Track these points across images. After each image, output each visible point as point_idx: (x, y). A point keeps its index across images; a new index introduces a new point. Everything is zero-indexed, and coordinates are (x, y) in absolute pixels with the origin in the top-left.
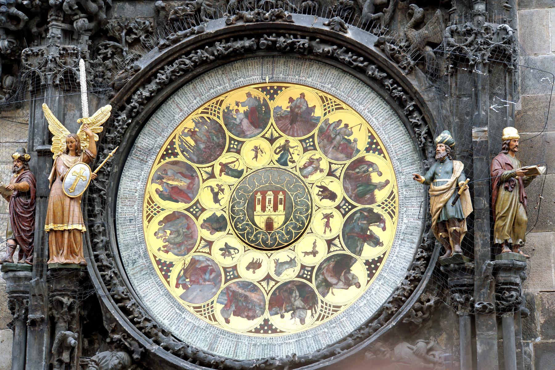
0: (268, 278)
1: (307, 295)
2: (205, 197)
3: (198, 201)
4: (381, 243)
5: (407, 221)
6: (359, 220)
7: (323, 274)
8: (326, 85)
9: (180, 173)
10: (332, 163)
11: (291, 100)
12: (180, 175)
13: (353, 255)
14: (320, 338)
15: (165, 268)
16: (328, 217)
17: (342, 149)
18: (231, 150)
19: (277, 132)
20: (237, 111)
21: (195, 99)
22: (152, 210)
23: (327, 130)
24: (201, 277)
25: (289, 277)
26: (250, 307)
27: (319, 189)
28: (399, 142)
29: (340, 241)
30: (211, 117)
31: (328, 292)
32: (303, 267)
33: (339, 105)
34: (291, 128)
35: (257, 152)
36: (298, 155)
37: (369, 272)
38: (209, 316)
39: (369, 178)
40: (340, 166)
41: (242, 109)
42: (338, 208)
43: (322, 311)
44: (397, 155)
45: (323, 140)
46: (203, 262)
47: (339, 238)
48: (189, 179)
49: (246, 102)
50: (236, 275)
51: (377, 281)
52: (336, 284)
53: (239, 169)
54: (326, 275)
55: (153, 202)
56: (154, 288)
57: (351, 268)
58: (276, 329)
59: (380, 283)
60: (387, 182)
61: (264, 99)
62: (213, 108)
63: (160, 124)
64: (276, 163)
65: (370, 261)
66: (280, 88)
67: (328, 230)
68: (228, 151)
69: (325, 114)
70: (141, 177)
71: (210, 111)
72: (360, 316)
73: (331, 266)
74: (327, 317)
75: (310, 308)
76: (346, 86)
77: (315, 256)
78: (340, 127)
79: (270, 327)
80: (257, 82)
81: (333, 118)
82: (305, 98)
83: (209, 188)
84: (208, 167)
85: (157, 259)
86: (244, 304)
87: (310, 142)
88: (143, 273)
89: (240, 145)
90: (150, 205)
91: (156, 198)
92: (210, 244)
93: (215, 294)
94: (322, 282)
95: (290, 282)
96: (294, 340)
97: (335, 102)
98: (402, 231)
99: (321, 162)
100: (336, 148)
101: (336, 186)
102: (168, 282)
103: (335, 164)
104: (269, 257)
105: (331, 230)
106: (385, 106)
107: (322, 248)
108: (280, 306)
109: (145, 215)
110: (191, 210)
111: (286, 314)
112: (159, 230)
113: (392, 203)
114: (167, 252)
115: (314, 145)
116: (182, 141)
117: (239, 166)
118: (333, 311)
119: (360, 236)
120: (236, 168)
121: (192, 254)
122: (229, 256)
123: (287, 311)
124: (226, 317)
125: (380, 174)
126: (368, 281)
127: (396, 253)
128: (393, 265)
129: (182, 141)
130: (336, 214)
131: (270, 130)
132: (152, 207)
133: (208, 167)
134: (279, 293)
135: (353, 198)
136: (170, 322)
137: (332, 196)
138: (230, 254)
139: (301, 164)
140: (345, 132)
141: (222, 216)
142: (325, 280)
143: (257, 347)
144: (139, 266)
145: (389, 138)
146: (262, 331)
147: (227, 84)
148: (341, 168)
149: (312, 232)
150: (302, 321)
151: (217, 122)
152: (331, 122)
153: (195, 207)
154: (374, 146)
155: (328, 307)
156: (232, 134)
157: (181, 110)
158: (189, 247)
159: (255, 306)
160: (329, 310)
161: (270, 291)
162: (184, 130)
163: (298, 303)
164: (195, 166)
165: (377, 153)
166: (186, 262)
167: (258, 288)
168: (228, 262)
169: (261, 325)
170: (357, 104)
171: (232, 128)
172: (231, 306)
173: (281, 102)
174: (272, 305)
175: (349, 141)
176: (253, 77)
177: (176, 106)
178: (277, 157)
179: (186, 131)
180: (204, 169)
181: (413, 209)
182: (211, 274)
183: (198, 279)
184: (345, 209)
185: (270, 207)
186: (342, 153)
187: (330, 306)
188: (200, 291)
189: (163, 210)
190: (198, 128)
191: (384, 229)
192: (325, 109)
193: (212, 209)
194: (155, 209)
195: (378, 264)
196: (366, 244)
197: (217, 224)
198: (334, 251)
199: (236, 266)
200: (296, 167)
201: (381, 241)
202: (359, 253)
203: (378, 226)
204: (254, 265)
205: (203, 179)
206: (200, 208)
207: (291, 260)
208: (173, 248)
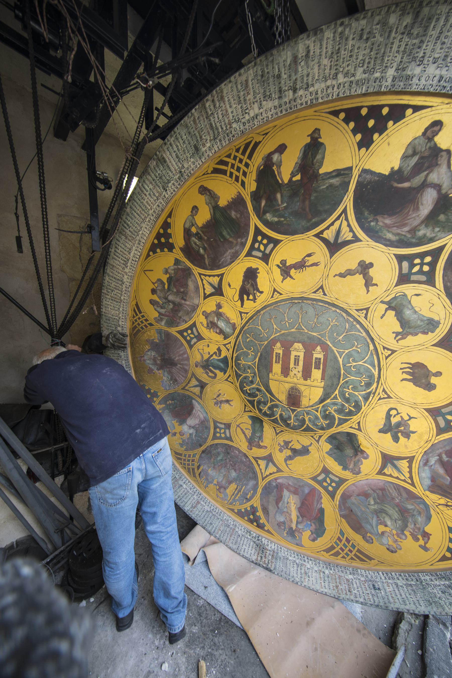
2: (304, 469)
3: (314, 479)
5: (256, 106)
6: (278, 210)
7: (414, 230)
9: (277, 502)
13: (352, 186)
21: (181, 486)
23: (167, 316)
25: (435, 300)
28: (145, 202)
29: (328, 228)
30: (196, 464)
32: (403, 279)
34: (180, 364)
35: (221, 402)
36: (208, 346)
40: (205, 282)
42: (266, 258)
44: (160, 195)
45: (180, 317)
47: (322, 232)
51: (415, 80)
53: (250, 422)
60: (203, 190)
64: (227, 374)
67: (311, 260)
70: (297, 561)
73: (388, 221)
76: (112, 308)
77: (371, 265)
83: (288, 462)
89: (218, 424)
92: (388, 459)
94: (437, 223)
100: (184, 295)
101: (234, 275)
103: (204, 289)
104: (393, 352)
105: (309, 255)
107: (348, 258)
113: (231, 161)
114: (426, 536)
115: (191, 328)
120: (250, 427)
125: (195, 209)
127: (329, 83)
133: (259, 465)
137: (251, 275)
139: (220, 338)
148: (207, 278)
149: (322, 287)
151: (200, 457)
154: (163, 240)
156: (208, 436)
158: (405, 495)
164: (262, 484)
170: (124, 286)
175: (170, 280)
180: (263, 471)
181: (230, 110)
184: (266, 246)
185: (297, 371)
186: (186, 285)
190: (213, 480)
196: (321, 171)
198: (351, 230)
199: (429, 411)
200: (225, 345)
201: (308, 140)
203: (279, 165)
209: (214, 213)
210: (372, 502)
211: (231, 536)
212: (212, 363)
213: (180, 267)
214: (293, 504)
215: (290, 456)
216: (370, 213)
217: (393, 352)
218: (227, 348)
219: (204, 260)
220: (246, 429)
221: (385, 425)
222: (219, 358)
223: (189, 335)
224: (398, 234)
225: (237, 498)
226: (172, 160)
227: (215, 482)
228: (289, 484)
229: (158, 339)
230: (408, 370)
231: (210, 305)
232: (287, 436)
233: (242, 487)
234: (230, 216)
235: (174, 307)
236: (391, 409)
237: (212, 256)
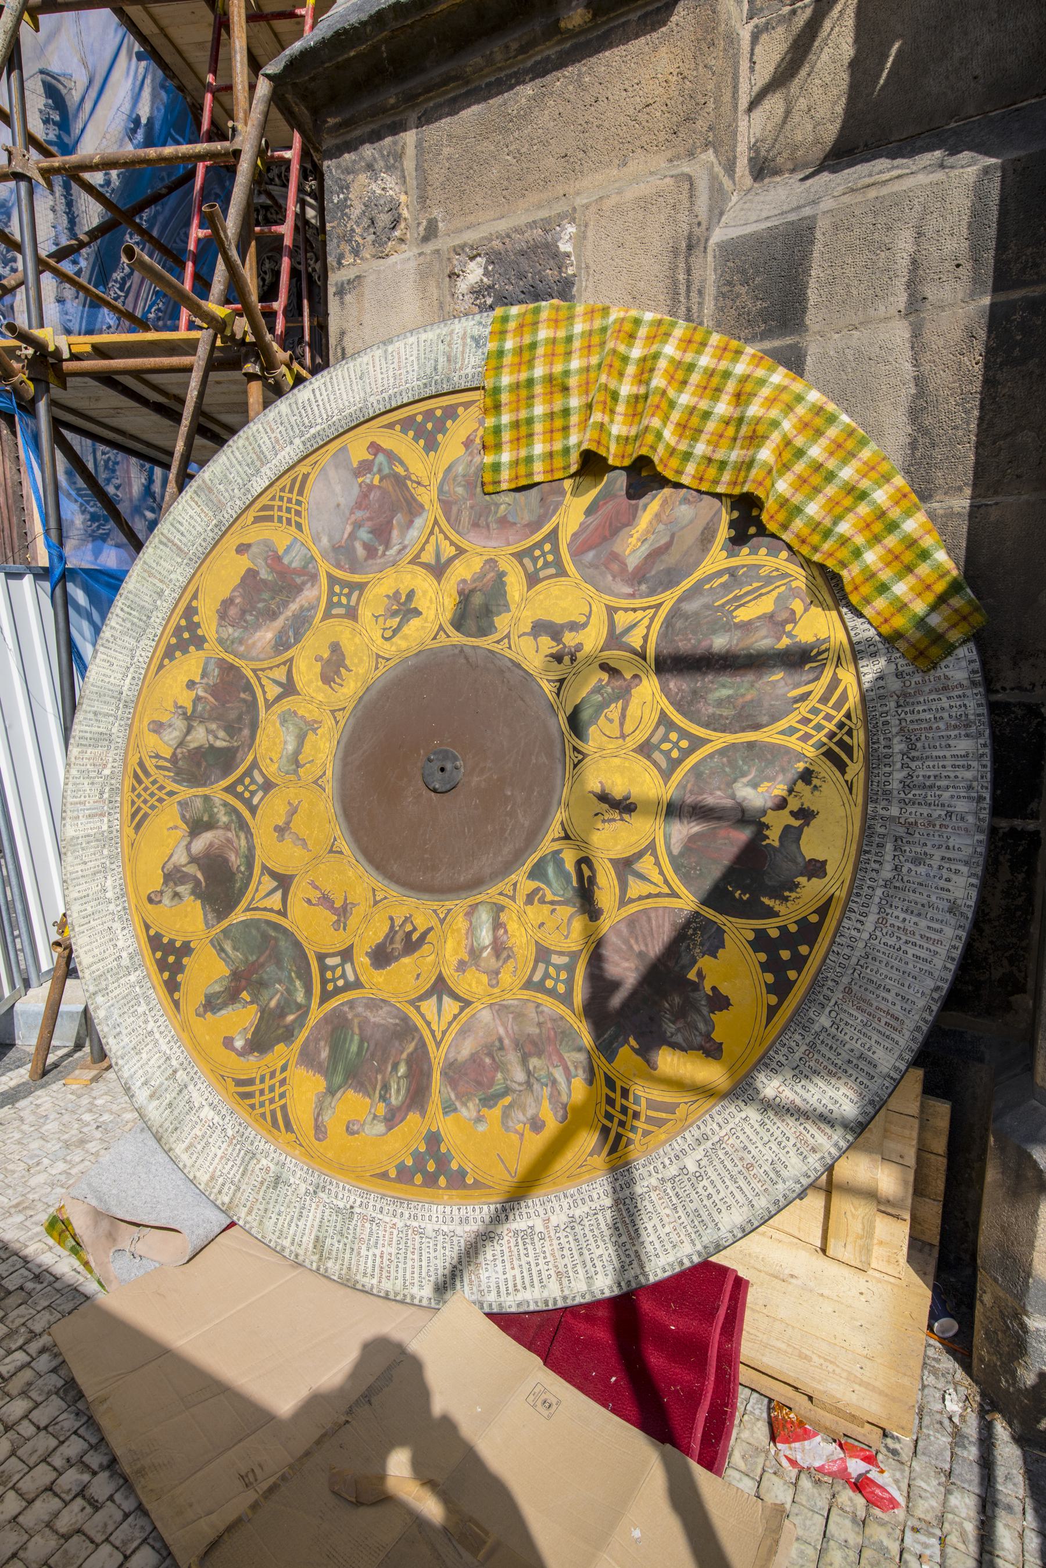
0: (289, 688)
1: (204, 764)
3: (562, 573)
4: (205, 1012)
6: (288, 990)
7: (227, 828)
8: (699, 1153)
9: (668, 546)
10: (462, 1009)
11: (720, 1002)
12: (663, 542)
13: (225, 923)
14: (99, 750)
15: (429, 426)
16: (343, 913)
17: (481, 1065)
18: (662, 730)
19: (641, 898)
23: (561, 1059)
24: (370, 519)
26: (249, 618)
27: (421, 929)
28: (394, 1251)
30: (803, 708)
31: (183, 817)
32: (268, 786)
34: (631, 947)
38: (271, 508)
42: (347, 955)
44: (364, 1217)
45: (540, 1025)
46: (403, 535)
47: (279, 912)
48: (638, 569)
49: (794, 847)
50: (334, 612)
53: (592, 730)
54: (220, 832)
56: (392, 380)
57: (199, 902)
59: (124, 954)
61: (771, 913)
66: (781, 988)
68: (663, 716)
71: (827, 709)
73: (233, 857)
78: (546, 1104)
79: (182, 646)
80: (846, 923)
83: (583, 619)
85: (460, 410)
86: (260, 605)
88: (442, 360)
92: (438, 570)
93: (316, 539)
94: (212, 816)
95: (253, 736)
96: (125, 689)
98: (191, 1087)
99: (485, 978)
100: (494, 1049)
102: (390, 426)
104: (333, 712)
106: (520, 1297)
108: (214, 690)
110: (547, 547)
115: (540, 987)
116: (769, 580)
118: (139, 809)
119: (253, 968)
121: (433, 510)
122: (387, 609)
124: (254, 549)
128: (140, 1010)
129: (769, 580)
130: (337, 941)
134: (244, 701)
135: (346, 1009)
136: (300, 405)
137: (381, 957)
142: (210, 826)
143: (155, 596)
144: (463, 352)
145: (421, 1233)
146: (183, 623)
147: (894, 811)
150: (158, 727)
151: (774, 719)
153: (550, 558)
154: (431, 1167)
155: (153, 801)
156: (711, 756)
158: (455, 509)
159: (246, 628)
161: (259, 679)
163: (200, 736)
164: (669, 598)
166: (421, 489)
168: (373, 602)
169: (198, 625)
171: (732, 763)
172: (272, 570)
174: (228, 670)
175: (489, 1101)
176: (872, 918)
180: (646, 622)
181: (220, 1153)
182: (366, 546)
183: (366, 508)
186: (474, 1058)
187: (153, 807)
193: (524, 605)
200: (513, 898)
204: (333, 667)
205: (616, 610)
209: (339, 1088)
210: (503, 507)
212: (564, 889)
213: (453, 1096)
214: (635, 536)
215: (571, 630)
216: (235, 881)
217: (333, 712)
218: (515, 890)
219: (412, 1053)
220: (611, 721)
222: (543, 886)
223: (557, 980)
224: (238, 836)
225: (755, 585)
226: (309, 1224)
228: (614, 577)
229: (627, 1041)
230: (337, 680)
233: (723, 605)
234: (330, 1057)
235: (531, 1055)
236: (387, 639)
237: (397, 1044)
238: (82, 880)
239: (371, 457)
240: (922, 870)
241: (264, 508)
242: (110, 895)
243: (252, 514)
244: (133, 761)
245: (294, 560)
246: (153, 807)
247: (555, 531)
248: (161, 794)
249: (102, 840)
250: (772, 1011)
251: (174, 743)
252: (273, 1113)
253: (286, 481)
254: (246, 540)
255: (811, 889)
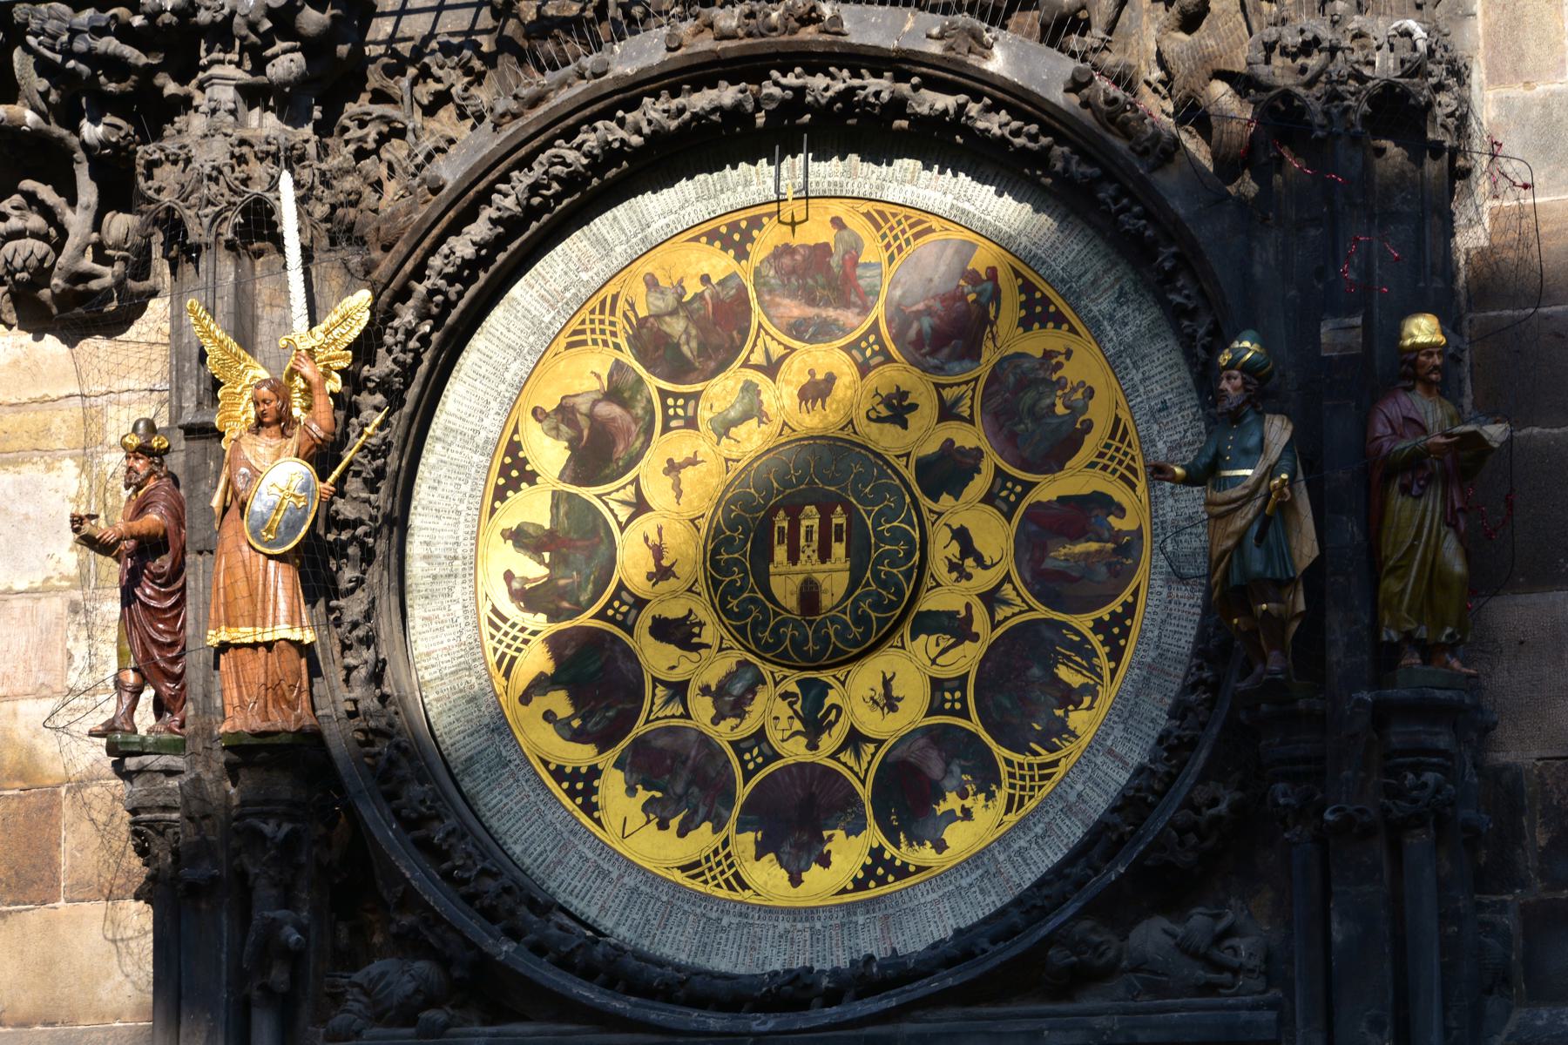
0: (771, 369)
1: (660, 352)
2: (995, 537)
7: (636, 420)
8: (735, 920)
9: (1074, 580)
11: (825, 861)
13: (573, 489)
14: (593, 251)
15: (1038, 309)
19: (845, 764)
20: (963, 795)
21: (1079, 795)
22: (1119, 456)
26: (793, 280)
29: (615, 516)
30: (1031, 759)
31: (610, 376)
32: (691, 423)
33: (693, 877)
36: (776, 718)
37: (521, 454)
38: (886, 220)
39: (575, 699)
40: (661, 714)
41: (952, 802)
43: (612, 324)
44: (513, 774)
46: (950, 358)
47: (619, 523)
52: (595, 402)
53: (923, 637)
54: (628, 418)
55: (1122, 477)
58: (710, 242)
59: (483, 434)
62: (1028, 783)
63: (1159, 697)
64: (832, 681)
65: (524, 485)
66: (860, 885)
68: (965, 677)
69: (726, 843)
72: (510, 335)
73: (621, 447)
74: (592, 312)
75: (642, 322)
77: (670, 461)
78: (680, 817)
81: (703, 839)
82: (786, 876)
83: (988, 562)
84: (1006, 619)
86: (810, 281)
87: (753, 759)
90: (1129, 468)
91: (1119, 493)
92: (947, 412)
93: (894, 284)
94: (633, 398)
95: (714, 374)
96: (654, 226)
97: (706, 882)
98: (459, 580)
99: (713, 712)
100: (679, 758)
101: (657, 658)
103: (673, 716)
104: (785, 424)
105: (646, 539)
106: (570, 899)
107: (657, 490)
108: (718, 304)
109: (1132, 435)
110: (1019, 489)
111: (700, 288)
112: (1086, 407)
113: (502, 648)
114: (1048, 355)
115: (740, 755)
116: (1092, 669)
117: (925, 645)
120: (933, 638)
121: (983, 370)
123: (699, 297)
124: (845, 233)
125: (549, 716)
126: (516, 431)
127: (462, 519)
129: (1092, 669)
131: (864, 766)
132: (1121, 462)
133: (1006, 619)
134: (733, 340)
138: (887, 402)
140: (664, 807)
141: (936, 499)
142: (625, 404)
143: (742, 180)
145: (542, 815)
147: (1001, 858)
148: (655, 708)
150: (652, 283)
152: (707, 827)
154: (580, 786)
157: (1110, 752)
158: (993, 389)
159: (784, 285)
160: (593, 331)
161: (758, 336)
162: (1093, 702)
163: (676, 327)
164: (1042, 612)
165: (568, 770)
166: (990, 344)
167: (789, 334)
169: (752, 240)
172: (843, 266)
173: (847, 853)
175: (647, 788)
176: (935, 896)
177: (1128, 760)
178: (832, 697)
179: (1087, 701)
180: (1017, 610)
181: (446, 644)
182: (919, 333)
185: (809, 551)
186: (661, 752)
188: (931, 280)
189: (1092, 465)
191: (509, 576)
192: (728, 856)
193: (968, 510)
194: (1112, 458)
195: (502, 481)
196: (547, 526)
197: (945, 472)
198: (624, 487)
200: (776, 684)
201: (510, 542)
202: (557, 497)
203: (526, 580)
205: (1011, 581)
206: (998, 502)
207: (726, 433)
208: (1034, 370)
211: (1169, 674)
216: (607, 466)
217: (785, 424)
221: (894, 423)
227: (1059, 713)
231: (702, 709)
232: (938, 565)
236: (869, 418)
238: (495, 341)
239: (984, 277)
240: (980, 897)
241: (881, 213)
242: (508, 376)
243: (866, 207)
244: (610, 290)
245: (865, 279)
246: (595, 342)
247: (1034, 484)
248: (610, 340)
249: (537, 327)
250: (844, 891)
251: (654, 310)
252: (504, 655)
253: (916, 216)
254: (846, 220)
255: (926, 854)
